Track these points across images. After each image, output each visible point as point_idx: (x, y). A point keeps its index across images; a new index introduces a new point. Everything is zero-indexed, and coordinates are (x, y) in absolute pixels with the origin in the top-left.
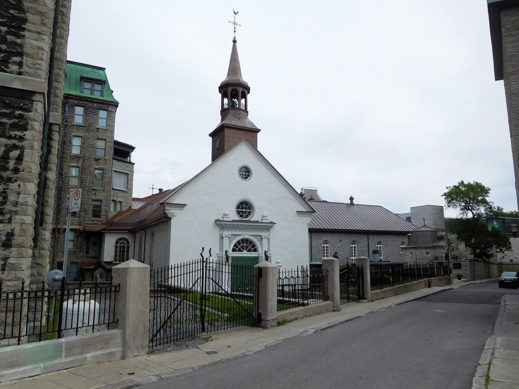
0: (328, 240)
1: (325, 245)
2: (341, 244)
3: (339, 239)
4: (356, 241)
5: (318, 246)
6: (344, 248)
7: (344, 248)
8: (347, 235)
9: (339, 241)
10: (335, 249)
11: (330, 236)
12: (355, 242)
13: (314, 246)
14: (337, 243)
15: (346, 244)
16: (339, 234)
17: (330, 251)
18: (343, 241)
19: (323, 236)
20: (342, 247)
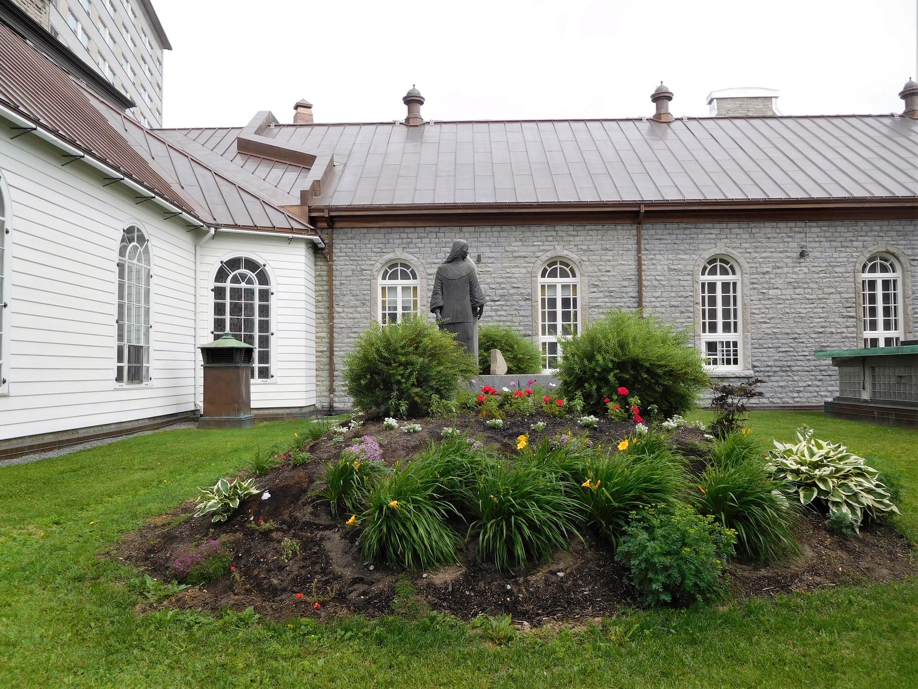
0: (735, 253)
1: (719, 279)
2: (806, 270)
3: (794, 247)
4: (893, 254)
5: (673, 283)
6: (826, 290)
7: (826, 290)
8: (839, 229)
9: (795, 255)
10: (771, 292)
11: (747, 236)
12: (893, 260)
13: (656, 283)
14: (779, 268)
15: (837, 269)
16: (792, 224)
17: (744, 304)
18: (818, 254)
19: (702, 236)
20: (811, 285)
